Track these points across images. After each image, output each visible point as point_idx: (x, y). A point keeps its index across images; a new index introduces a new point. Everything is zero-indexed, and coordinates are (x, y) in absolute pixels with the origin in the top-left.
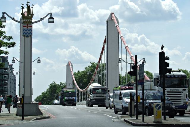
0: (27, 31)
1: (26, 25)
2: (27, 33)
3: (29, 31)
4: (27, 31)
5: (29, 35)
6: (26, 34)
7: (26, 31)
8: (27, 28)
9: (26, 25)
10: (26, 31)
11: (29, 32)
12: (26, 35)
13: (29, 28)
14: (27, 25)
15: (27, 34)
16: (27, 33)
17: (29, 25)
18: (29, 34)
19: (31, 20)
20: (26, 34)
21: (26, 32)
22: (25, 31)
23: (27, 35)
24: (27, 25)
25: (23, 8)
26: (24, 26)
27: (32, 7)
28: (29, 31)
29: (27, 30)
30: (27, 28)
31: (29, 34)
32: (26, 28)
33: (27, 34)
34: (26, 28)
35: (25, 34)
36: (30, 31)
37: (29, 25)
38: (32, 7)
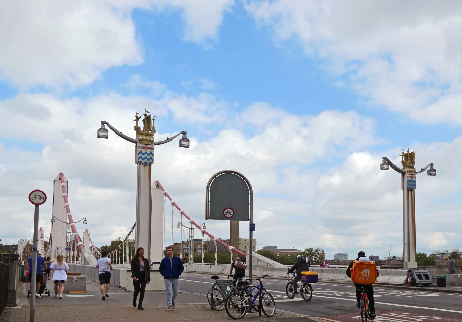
2: (146, 158)
7: (143, 154)
11: (148, 157)
12: (143, 162)
17: (148, 146)
19: (152, 139)
21: (143, 157)
25: (138, 119)
27: (153, 120)
29: (146, 153)
31: (148, 160)
36: (151, 156)
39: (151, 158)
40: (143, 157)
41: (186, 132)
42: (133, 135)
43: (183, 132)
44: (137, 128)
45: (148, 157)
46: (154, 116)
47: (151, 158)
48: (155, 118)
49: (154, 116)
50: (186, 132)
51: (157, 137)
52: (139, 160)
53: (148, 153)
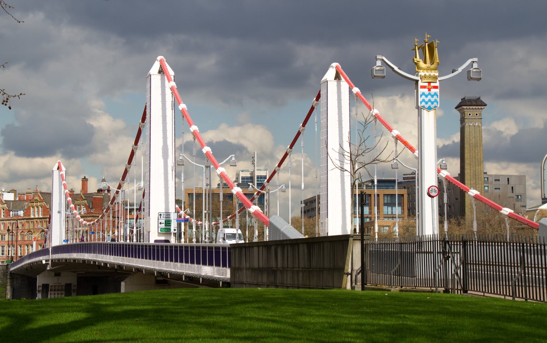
0: (429, 97)
1: (426, 84)
2: (430, 100)
3: (432, 96)
4: (429, 97)
5: (432, 106)
6: (427, 103)
7: (426, 96)
8: (429, 90)
10: (426, 96)
12: (427, 106)
15: (429, 103)
17: (432, 84)
18: (432, 103)
21: (427, 100)
24: (429, 83)
28: (432, 96)
29: (429, 94)
30: (429, 90)
31: (432, 103)
32: (427, 90)
37: (432, 84)
40: (427, 100)
45: (433, 100)
53: (432, 94)
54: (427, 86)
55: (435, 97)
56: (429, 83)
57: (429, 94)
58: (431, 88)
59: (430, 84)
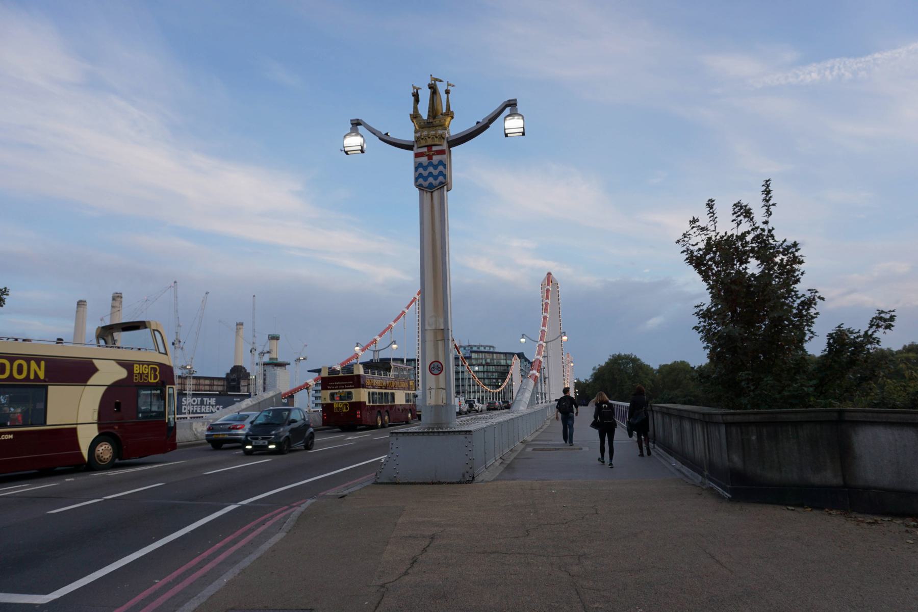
1: (425, 150)
3: (435, 167)
4: (431, 169)
5: (435, 183)
6: (425, 179)
7: (425, 168)
8: (430, 158)
9: (425, 150)
10: (425, 168)
11: (435, 173)
12: (426, 184)
13: (436, 159)
14: (429, 147)
15: (431, 180)
16: (430, 174)
17: (434, 148)
18: (436, 178)
20: (425, 179)
22: (421, 170)
23: (431, 184)
26: (417, 155)
27: (447, 92)
28: (435, 167)
29: (430, 164)
30: (430, 158)
31: (436, 178)
32: (426, 158)
33: (431, 180)
34: (424, 160)
35: (421, 181)
36: (441, 168)
37: (434, 148)
38: (447, 92)
39: (441, 173)
40: (425, 173)
41: (516, 100)
42: (408, 133)
43: (509, 101)
44: (415, 116)
46: (449, 85)
47: (441, 173)
48: (450, 88)
49: (449, 85)
50: (516, 100)
51: (455, 128)
52: (418, 183)
54: (425, 152)
55: (441, 168)
56: (429, 147)
57: (430, 164)
58: (434, 154)
59: (432, 148)
